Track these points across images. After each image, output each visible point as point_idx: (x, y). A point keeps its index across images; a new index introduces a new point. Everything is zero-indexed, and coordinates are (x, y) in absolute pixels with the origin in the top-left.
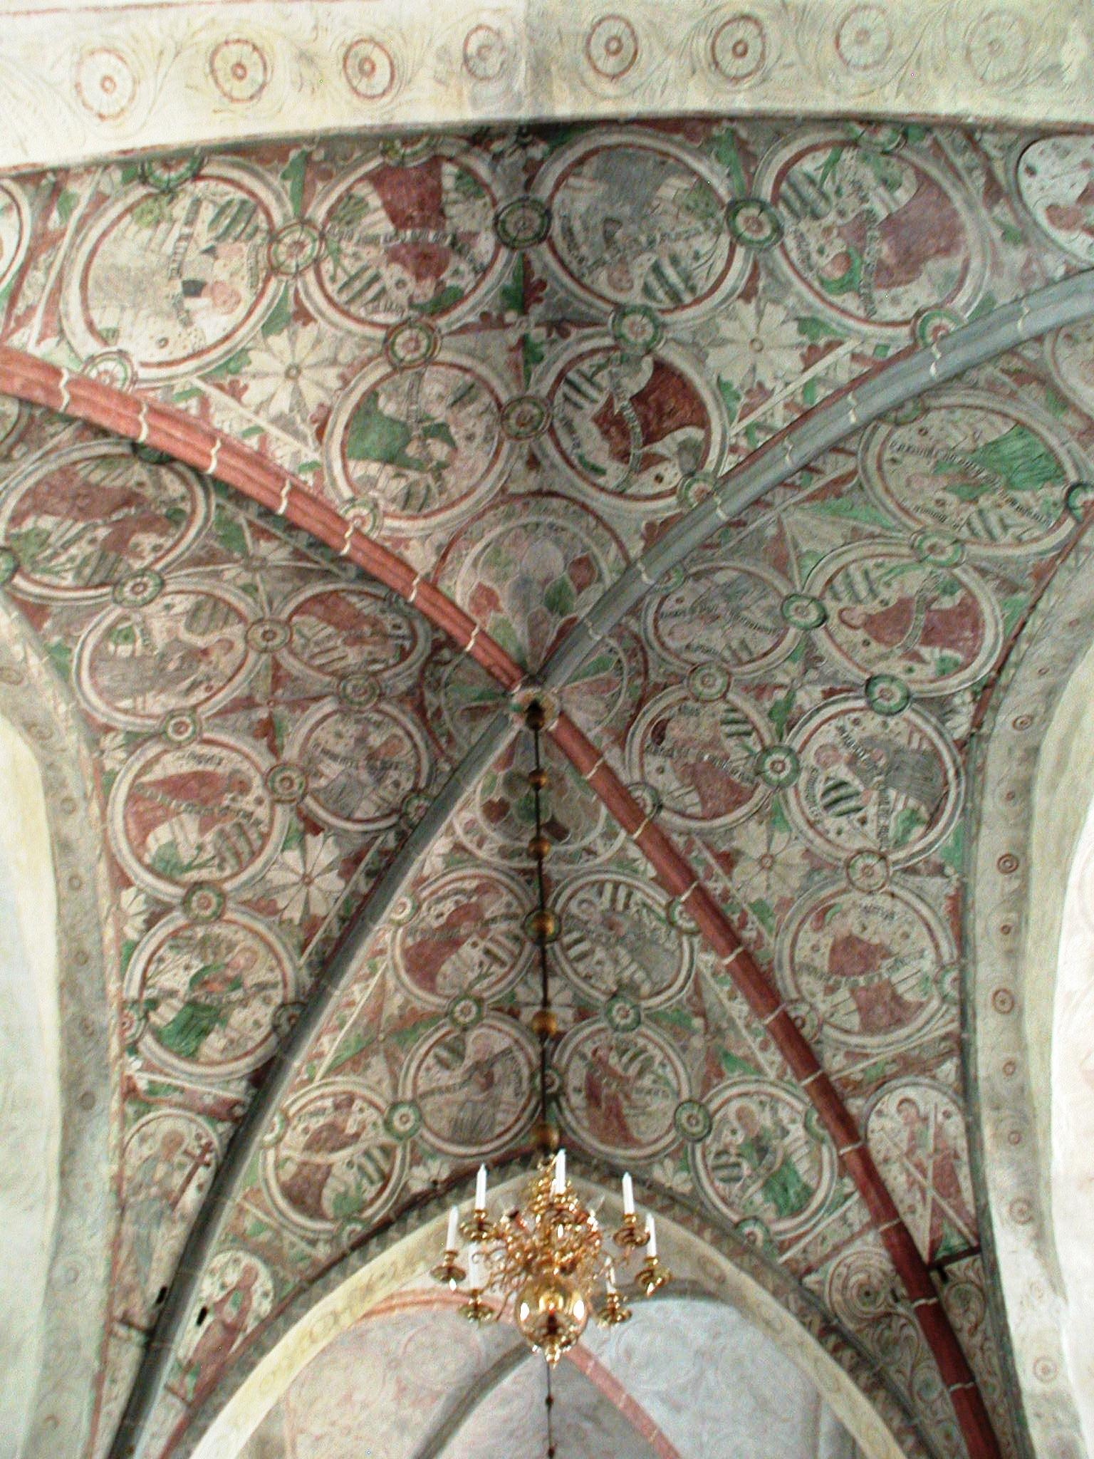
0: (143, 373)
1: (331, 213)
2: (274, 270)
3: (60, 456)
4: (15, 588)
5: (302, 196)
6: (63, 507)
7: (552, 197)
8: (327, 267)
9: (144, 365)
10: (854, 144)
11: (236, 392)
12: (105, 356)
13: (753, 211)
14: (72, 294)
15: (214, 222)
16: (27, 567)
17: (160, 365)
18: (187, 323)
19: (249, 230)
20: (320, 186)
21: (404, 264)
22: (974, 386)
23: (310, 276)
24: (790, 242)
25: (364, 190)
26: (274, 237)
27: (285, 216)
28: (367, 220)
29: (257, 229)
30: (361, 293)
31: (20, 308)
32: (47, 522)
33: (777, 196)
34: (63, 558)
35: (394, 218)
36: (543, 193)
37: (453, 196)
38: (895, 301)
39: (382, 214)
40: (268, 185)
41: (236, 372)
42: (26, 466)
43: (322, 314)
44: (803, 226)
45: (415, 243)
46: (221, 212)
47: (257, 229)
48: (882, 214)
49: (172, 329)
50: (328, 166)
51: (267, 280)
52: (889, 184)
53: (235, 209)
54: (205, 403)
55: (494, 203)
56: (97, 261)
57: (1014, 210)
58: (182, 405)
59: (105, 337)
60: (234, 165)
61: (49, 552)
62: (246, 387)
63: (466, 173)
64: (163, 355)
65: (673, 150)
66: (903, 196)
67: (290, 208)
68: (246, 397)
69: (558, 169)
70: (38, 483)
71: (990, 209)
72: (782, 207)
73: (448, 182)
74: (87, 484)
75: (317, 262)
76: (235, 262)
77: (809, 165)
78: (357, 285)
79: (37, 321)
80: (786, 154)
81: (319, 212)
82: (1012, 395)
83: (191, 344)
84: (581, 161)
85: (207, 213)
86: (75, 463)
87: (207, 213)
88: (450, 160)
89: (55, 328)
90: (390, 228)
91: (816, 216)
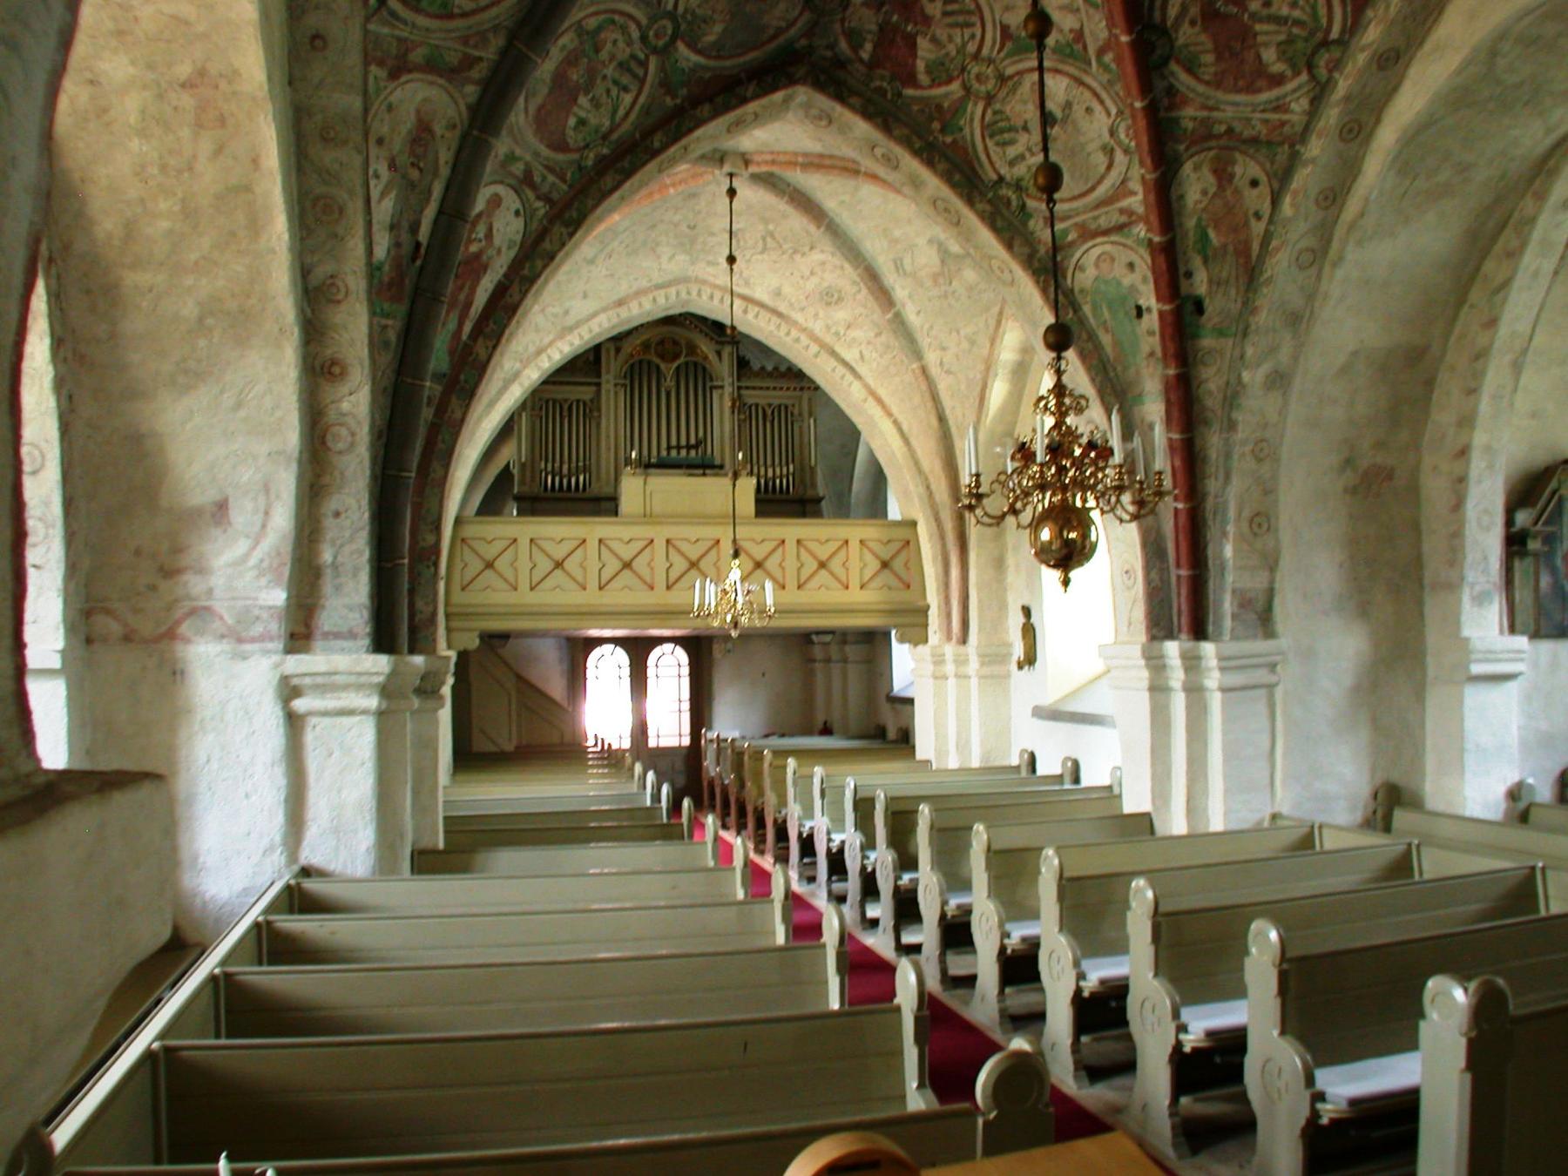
0: (1114, 111)
1: (950, 81)
2: (1002, 79)
3: (1208, 98)
4: (1343, 31)
5: (959, 107)
6: (1250, 56)
7: (801, 14)
8: (972, 48)
9: (1109, 114)
10: (605, 137)
11: (1079, 35)
12: (1119, 143)
13: (661, 43)
14: (1101, 191)
15: (1012, 142)
16: (1320, 35)
17: (1102, 102)
18: (1068, 105)
19: (998, 117)
20: (946, 105)
21: (922, 9)
22: (495, 29)
23: (985, 52)
24: (635, 34)
25: (923, 78)
26: (989, 99)
27: (976, 104)
28: (932, 56)
29: (995, 113)
30: (961, 12)
31: (1123, 219)
32: (1269, 55)
33: (644, 64)
34: (1297, 14)
35: (915, 44)
36: (807, 16)
37: (869, 37)
38: (564, 47)
39: (920, 53)
40: (972, 135)
41: (1068, 45)
42: (1229, 113)
43: (994, 21)
44: (628, 50)
45: (907, 21)
46: (1005, 144)
47: (995, 113)
48: (583, 100)
49: (1078, 111)
50: (936, 115)
51: (1011, 77)
52: (582, 122)
53: (997, 138)
54: (1101, 52)
55: (843, 21)
56: (1076, 192)
57: (516, 177)
58: (1113, 66)
59: (1109, 152)
60: (981, 166)
61: (1295, 30)
62: (1071, 31)
63: (856, 47)
64: (1097, 107)
65: (712, 63)
66: (572, 121)
67: (970, 106)
68: (1077, 26)
69: (792, 31)
70: (1239, 91)
71: (527, 164)
72: (642, 56)
73: (868, 46)
74: (1219, 58)
75: (976, 56)
76: (1018, 108)
77: (627, 99)
78: (961, 19)
79: (1125, 203)
80: (642, 99)
81: (955, 86)
82: (465, 41)
83: (1078, 92)
84: (774, 37)
85: (1012, 152)
86: (1207, 83)
87: (1012, 152)
88: (861, 60)
89: (1122, 190)
90: (919, 40)
91: (621, 65)
